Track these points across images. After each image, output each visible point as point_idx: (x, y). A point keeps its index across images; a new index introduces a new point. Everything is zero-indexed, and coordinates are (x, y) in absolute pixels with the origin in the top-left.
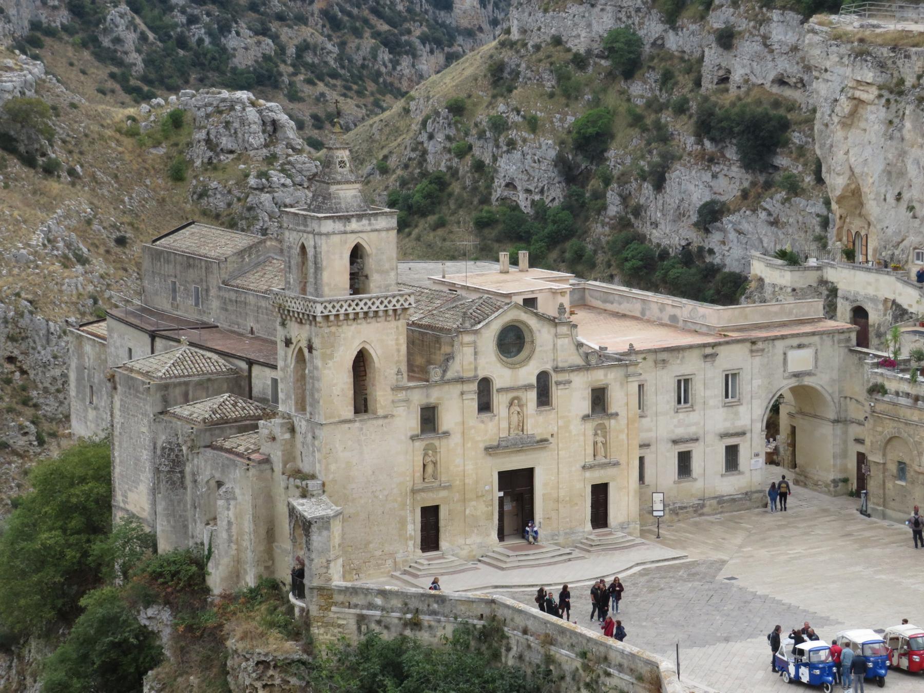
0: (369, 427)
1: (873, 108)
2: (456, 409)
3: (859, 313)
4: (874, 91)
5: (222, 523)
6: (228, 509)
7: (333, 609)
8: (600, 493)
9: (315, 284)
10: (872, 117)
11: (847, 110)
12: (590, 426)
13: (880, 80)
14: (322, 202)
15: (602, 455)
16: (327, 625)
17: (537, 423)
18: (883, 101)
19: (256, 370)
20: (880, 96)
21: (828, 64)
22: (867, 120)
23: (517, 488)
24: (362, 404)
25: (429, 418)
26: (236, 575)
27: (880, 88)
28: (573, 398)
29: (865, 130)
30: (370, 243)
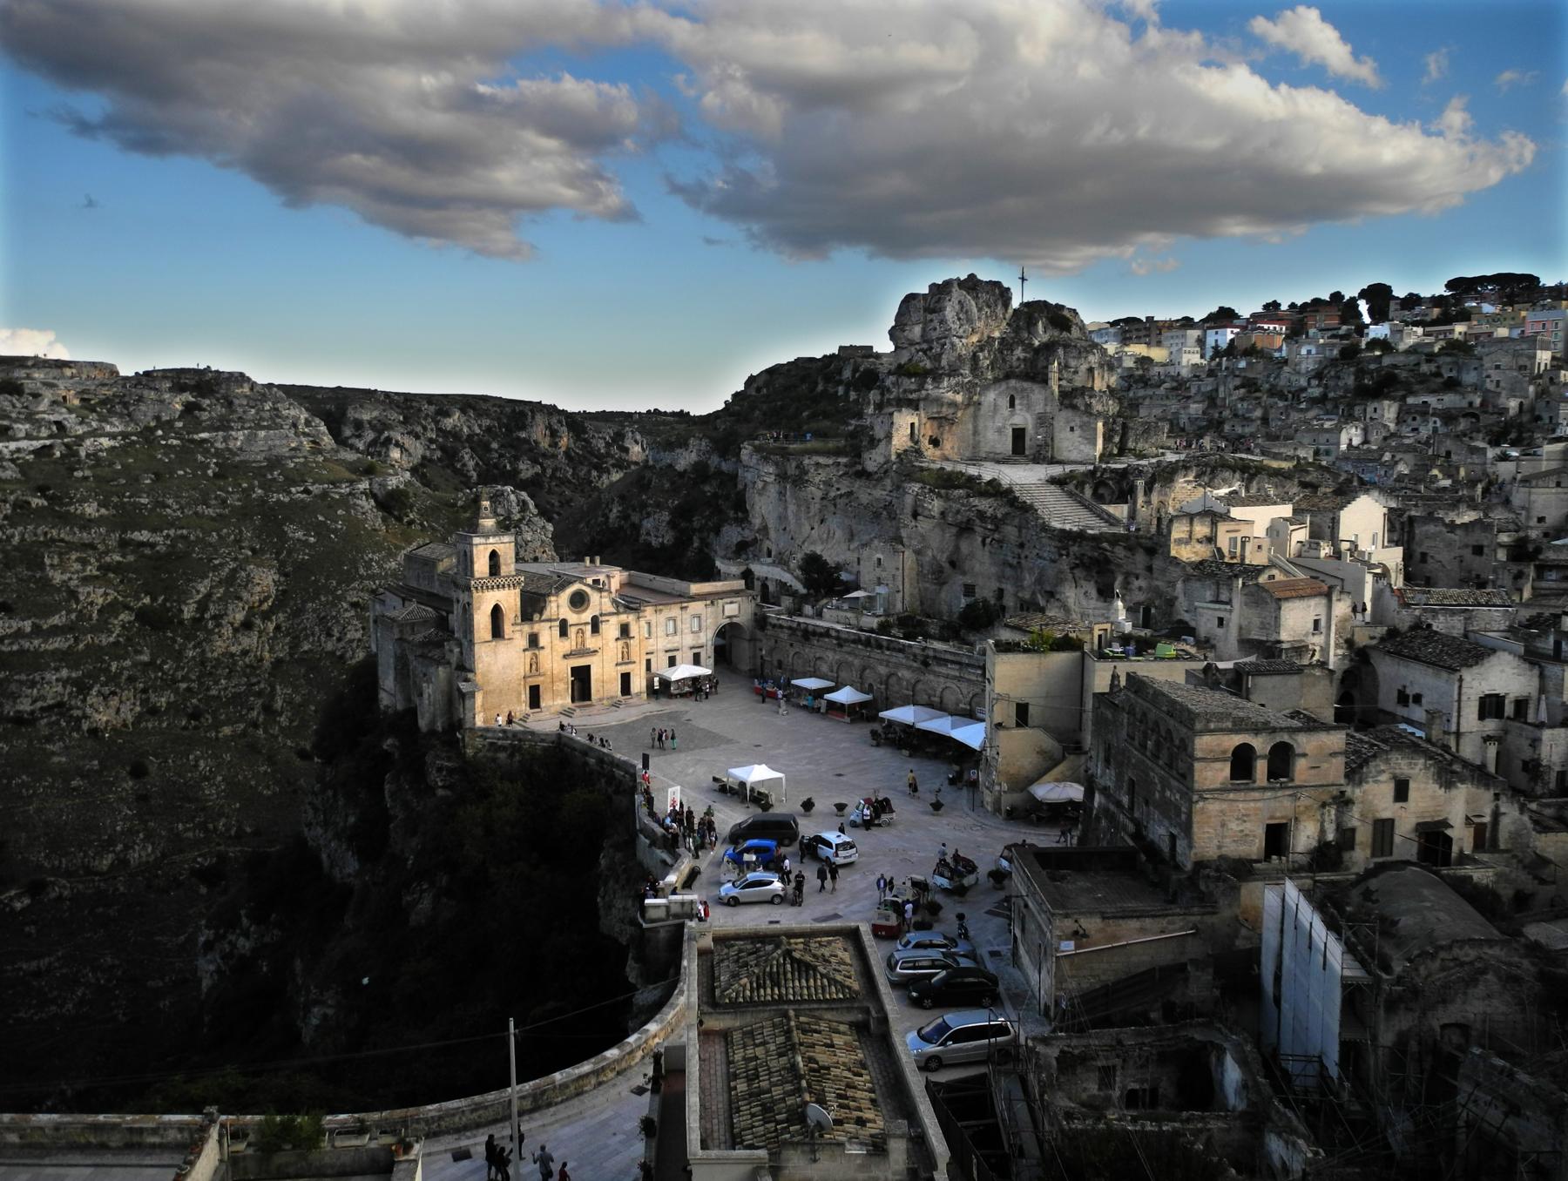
0: (501, 646)
2: (548, 634)
3: (765, 587)
8: (626, 678)
12: (620, 643)
14: (474, 528)
15: (626, 659)
17: (591, 642)
23: (581, 677)
24: (497, 632)
25: (534, 641)
26: (433, 722)
28: (611, 629)
30: (500, 549)
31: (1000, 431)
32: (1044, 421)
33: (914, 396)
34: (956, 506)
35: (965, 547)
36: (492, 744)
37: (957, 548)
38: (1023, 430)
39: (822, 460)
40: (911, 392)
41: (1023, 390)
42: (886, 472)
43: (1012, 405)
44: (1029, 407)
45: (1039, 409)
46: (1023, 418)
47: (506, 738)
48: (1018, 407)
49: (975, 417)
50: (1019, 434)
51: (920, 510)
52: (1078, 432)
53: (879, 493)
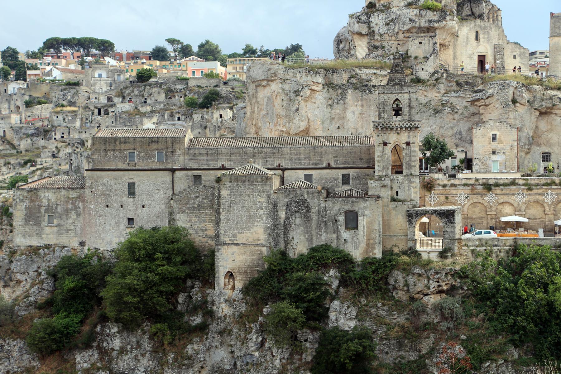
1: (321, 93)
4: (321, 87)
5: (360, 227)
6: (364, 221)
7: (463, 248)
9: (409, 115)
10: (319, 97)
11: (308, 94)
13: (323, 82)
16: (461, 255)
18: (326, 90)
19: (287, 173)
20: (324, 88)
21: (288, 77)
22: (315, 99)
27: (323, 85)
29: (315, 103)
31: (470, 57)
32: (498, 50)
33: (436, 25)
34: (539, 96)
35: (543, 125)
36: (473, 251)
37: (537, 127)
38: (484, 56)
39: (375, 71)
40: (436, 22)
41: (485, 28)
42: (437, 80)
43: (477, 38)
44: (489, 40)
45: (495, 41)
46: (486, 49)
47: (482, 245)
49: (455, 46)
50: (482, 61)
51: (518, 99)
52: (518, 59)
53: (433, 95)
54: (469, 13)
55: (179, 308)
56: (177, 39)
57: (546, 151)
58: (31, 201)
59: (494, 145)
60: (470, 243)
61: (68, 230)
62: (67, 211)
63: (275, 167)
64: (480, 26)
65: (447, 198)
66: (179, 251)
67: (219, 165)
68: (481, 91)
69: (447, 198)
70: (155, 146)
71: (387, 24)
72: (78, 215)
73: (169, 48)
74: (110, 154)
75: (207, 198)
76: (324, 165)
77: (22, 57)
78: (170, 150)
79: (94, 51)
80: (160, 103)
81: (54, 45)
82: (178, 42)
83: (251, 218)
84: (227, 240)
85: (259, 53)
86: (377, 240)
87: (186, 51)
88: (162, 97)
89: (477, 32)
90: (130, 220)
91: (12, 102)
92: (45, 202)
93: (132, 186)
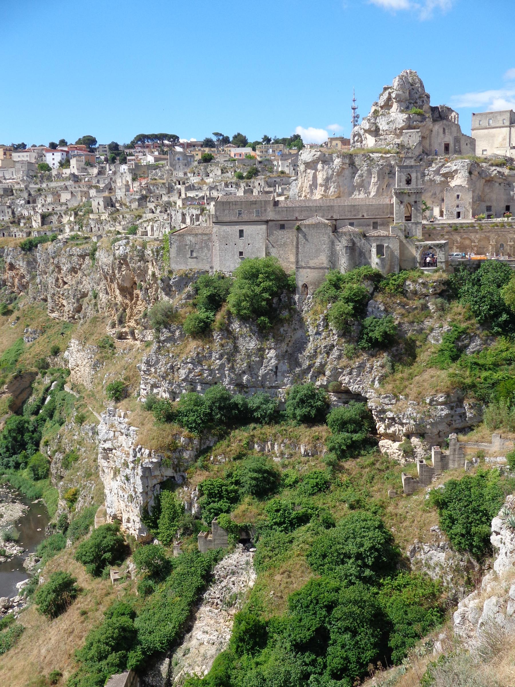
4: (348, 165)
19: (338, 222)
31: (440, 144)
37: (483, 190)
38: (448, 144)
41: (449, 125)
44: (451, 133)
45: (455, 134)
48: (447, 133)
49: (430, 137)
52: (469, 145)
54: (438, 115)
55: (274, 305)
56: (220, 132)
57: (489, 205)
58: (180, 242)
59: (457, 202)
60: (453, 264)
61: (203, 260)
62: (201, 248)
63: (329, 218)
64: (446, 125)
65: (430, 236)
66: (273, 273)
67: (294, 218)
68: (449, 167)
69: (430, 236)
70: (254, 206)
71: (388, 124)
72: (209, 250)
73: (214, 139)
74: (226, 212)
75: (289, 238)
76: (360, 217)
77: (121, 149)
78: (263, 209)
79: (166, 142)
80: (218, 176)
81: (142, 138)
82: (221, 135)
83: (318, 251)
84: (303, 265)
85: (272, 141)
86: (396, 263)
87: (225, 141)
88: (219, 172)
89: (444, 129)
90: (241, 253)
91: (124, 178)
92: (188, 243)
93: (241, 232)
